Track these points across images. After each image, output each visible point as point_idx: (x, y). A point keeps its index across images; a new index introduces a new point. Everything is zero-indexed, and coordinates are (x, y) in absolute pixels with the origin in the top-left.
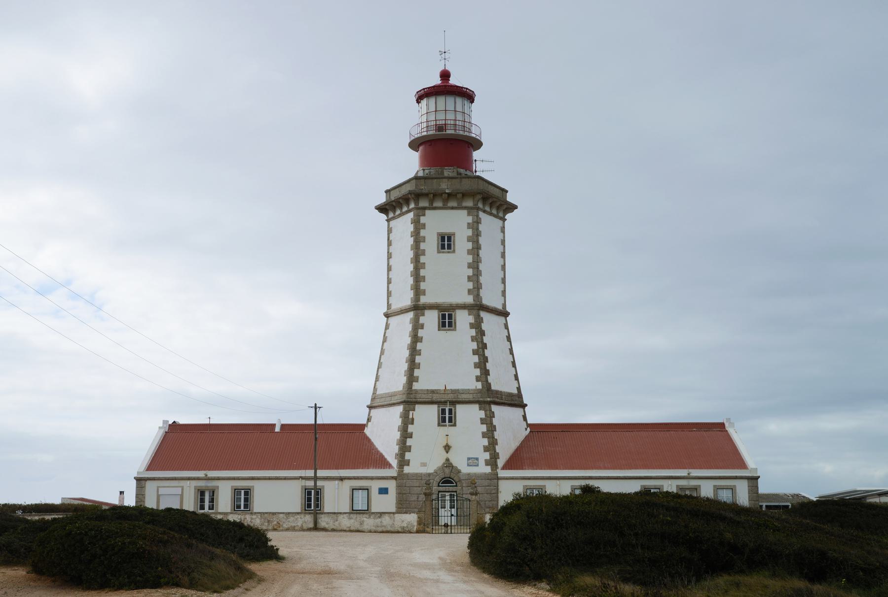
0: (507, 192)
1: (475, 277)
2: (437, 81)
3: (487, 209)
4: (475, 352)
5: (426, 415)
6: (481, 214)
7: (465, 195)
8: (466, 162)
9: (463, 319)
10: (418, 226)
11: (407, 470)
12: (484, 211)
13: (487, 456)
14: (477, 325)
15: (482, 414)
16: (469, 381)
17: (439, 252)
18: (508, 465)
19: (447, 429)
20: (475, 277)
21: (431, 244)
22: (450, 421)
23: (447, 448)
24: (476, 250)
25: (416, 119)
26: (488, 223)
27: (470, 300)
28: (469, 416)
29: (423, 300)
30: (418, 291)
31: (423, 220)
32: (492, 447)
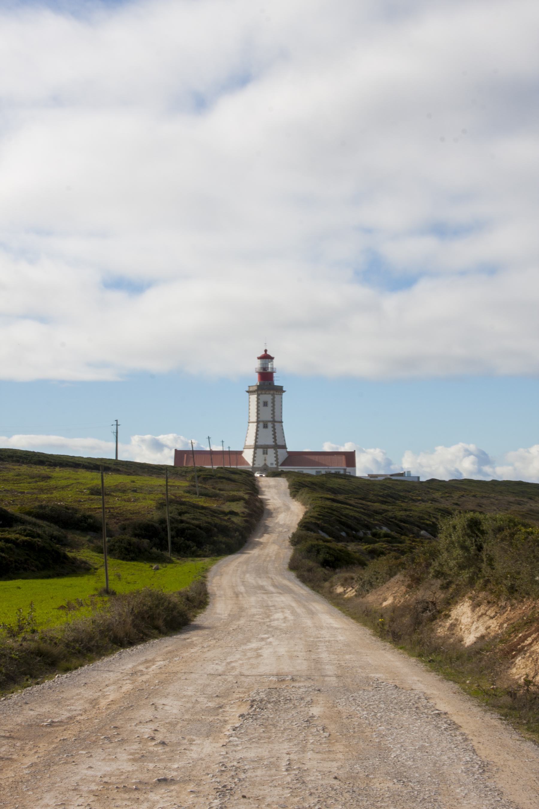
1: (273, 414)
5: (260, 451)
9: (270, 425)
11: (254, 466)
13: (275, 463)
15: (274, 451)
16: (271, 442)
19: (265, 455)
20: (273, 414)
23: (265, 460)
27: (272, 420)
28: (271, 452)
30: (258, 418)
32: (277, 460)
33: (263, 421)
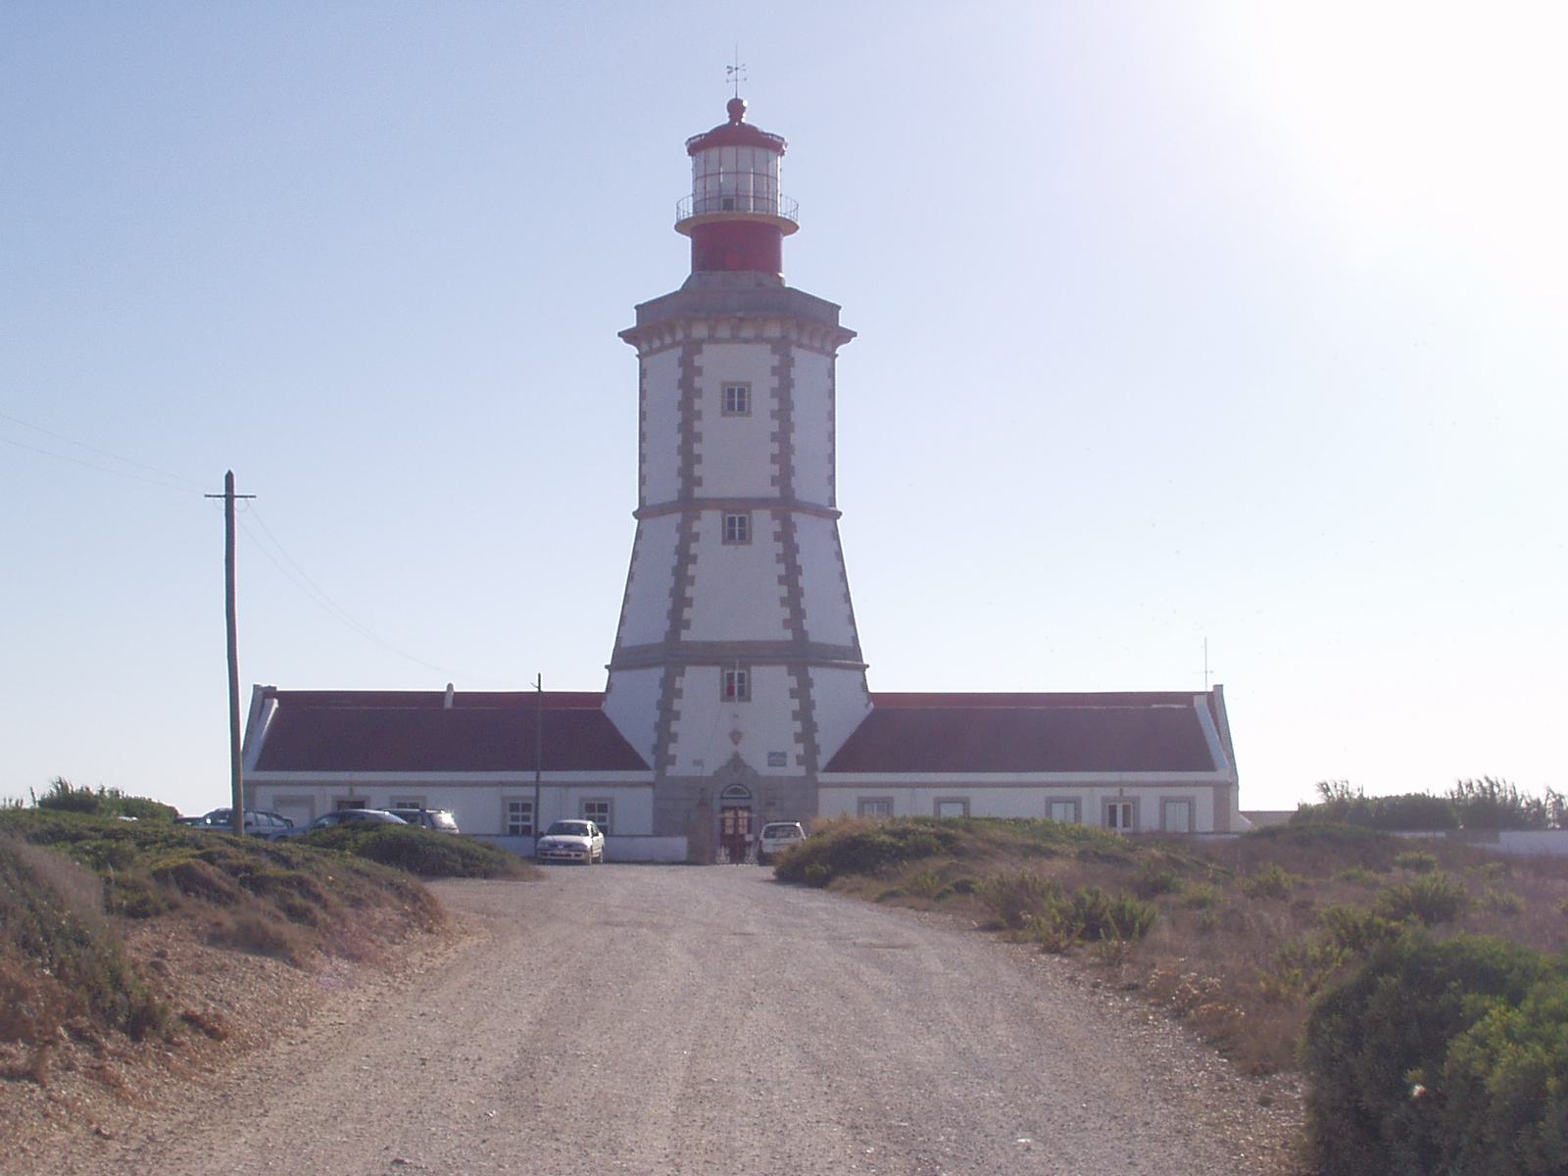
3: (805, 341)
4: (782, 580)
5: (701, 683)
8: (773, 263)
9: (763, 524)
10: (689, 374)
12: (800, 346)
13: (800, 749)
16: (770, 626)
17: (724, 414)
18: (834, 766)
21: (710, 403)
22: (741, 692)
23: (736, 736)
27: (775, 492)
29: (698, 492)
30: (689, 480)
31: (698, 361)
32: (807, 734)
33: (719, 503)
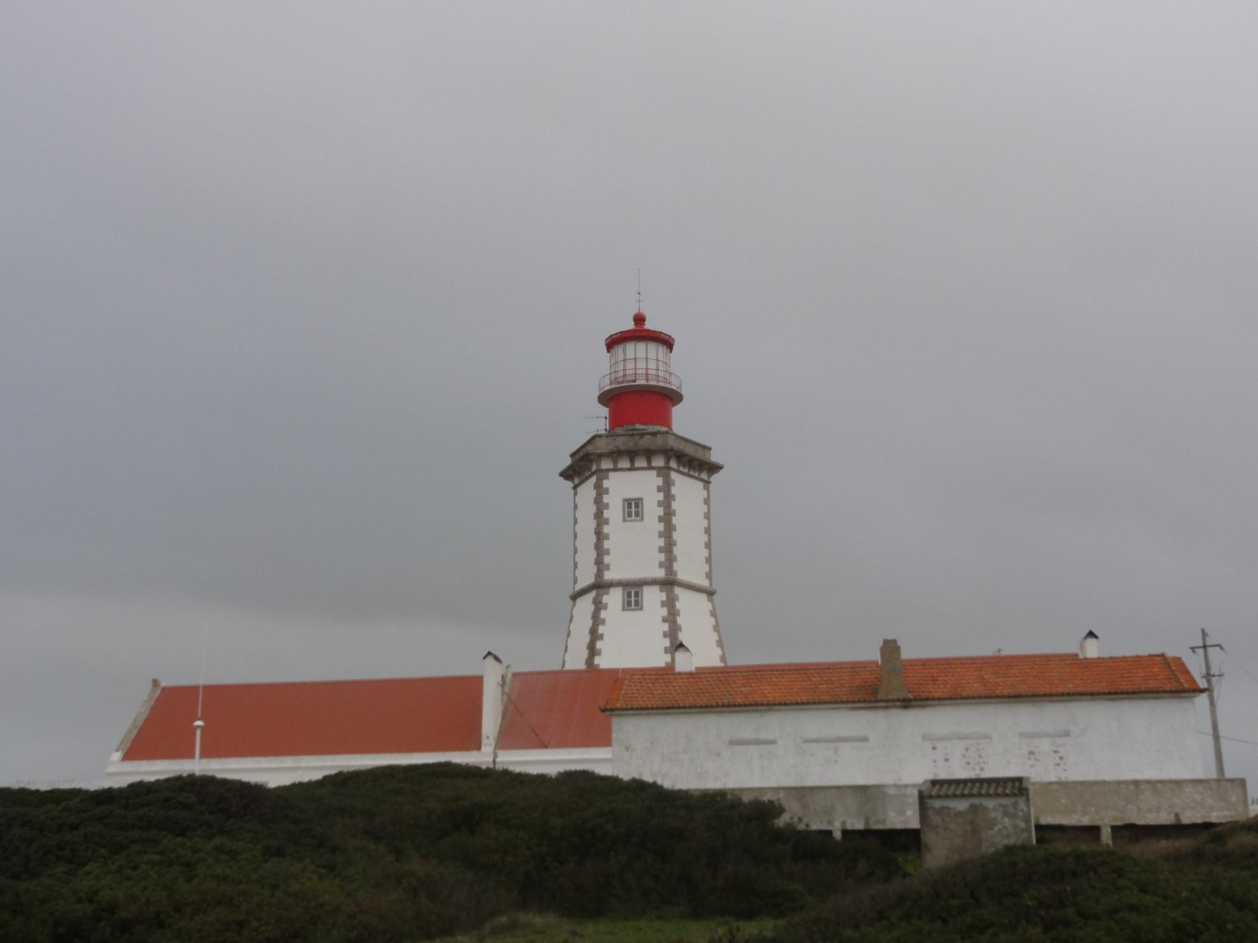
0: (710, 449)
1: (668, 549)
2: (630, 325)
6: (674, 475)
7: (649, 454)
9: (653, 597)
12: (678, 471)
14: (670, 603)
20: (668, 549)
21: (614, 512)
24: (667, 518)
25: (599, 370)
26: (686, 489)
27: (661, 574)
